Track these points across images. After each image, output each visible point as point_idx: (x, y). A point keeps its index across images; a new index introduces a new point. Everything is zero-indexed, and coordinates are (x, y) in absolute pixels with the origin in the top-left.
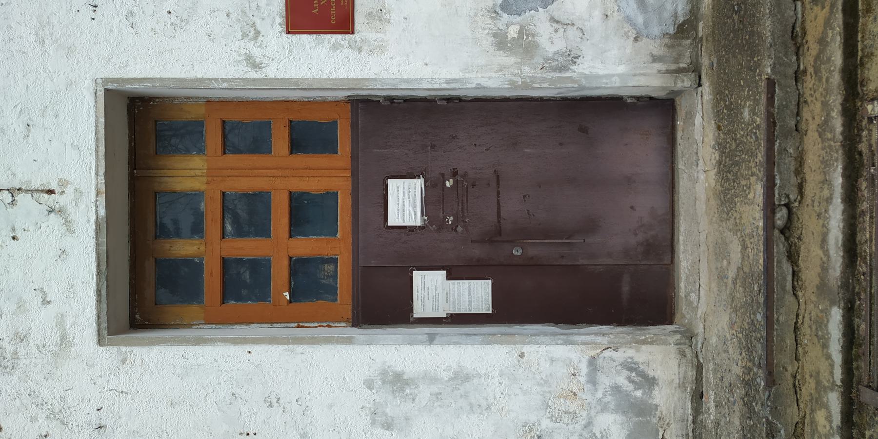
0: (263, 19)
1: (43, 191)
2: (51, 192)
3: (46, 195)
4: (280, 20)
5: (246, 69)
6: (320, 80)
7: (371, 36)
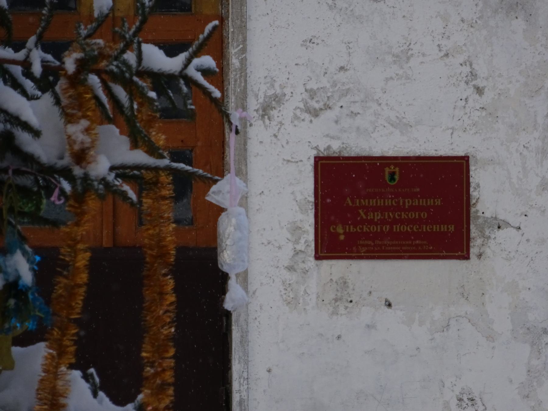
0: (337, 122)
5: (261, 95)
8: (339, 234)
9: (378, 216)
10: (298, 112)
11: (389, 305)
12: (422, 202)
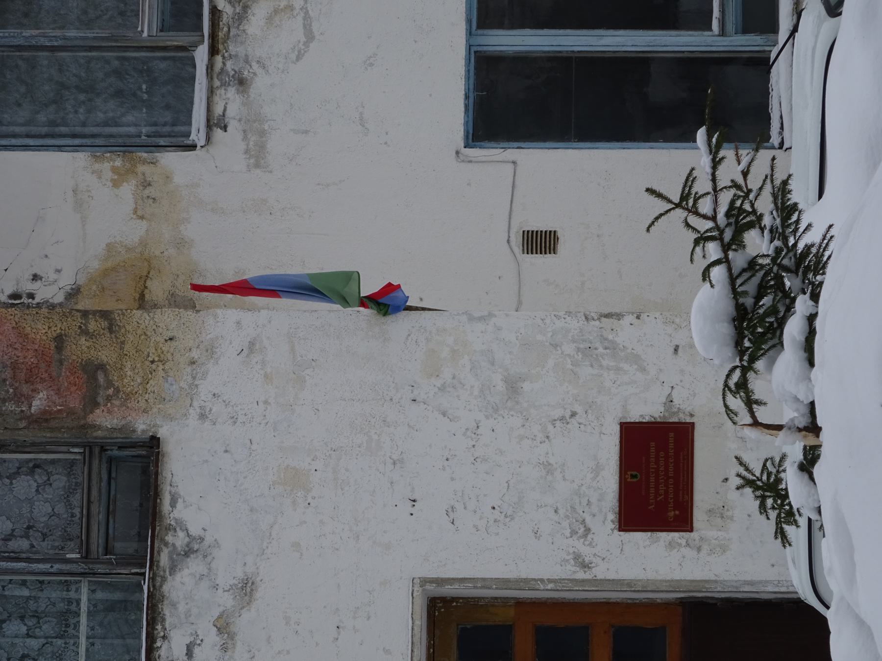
4: (612, 516)
5: (573, 569)
6: (654, 582)
8: (675, 514)
9: (662, 488)
10: (587, 543)
11: (727, 479)
12: (653, 455)
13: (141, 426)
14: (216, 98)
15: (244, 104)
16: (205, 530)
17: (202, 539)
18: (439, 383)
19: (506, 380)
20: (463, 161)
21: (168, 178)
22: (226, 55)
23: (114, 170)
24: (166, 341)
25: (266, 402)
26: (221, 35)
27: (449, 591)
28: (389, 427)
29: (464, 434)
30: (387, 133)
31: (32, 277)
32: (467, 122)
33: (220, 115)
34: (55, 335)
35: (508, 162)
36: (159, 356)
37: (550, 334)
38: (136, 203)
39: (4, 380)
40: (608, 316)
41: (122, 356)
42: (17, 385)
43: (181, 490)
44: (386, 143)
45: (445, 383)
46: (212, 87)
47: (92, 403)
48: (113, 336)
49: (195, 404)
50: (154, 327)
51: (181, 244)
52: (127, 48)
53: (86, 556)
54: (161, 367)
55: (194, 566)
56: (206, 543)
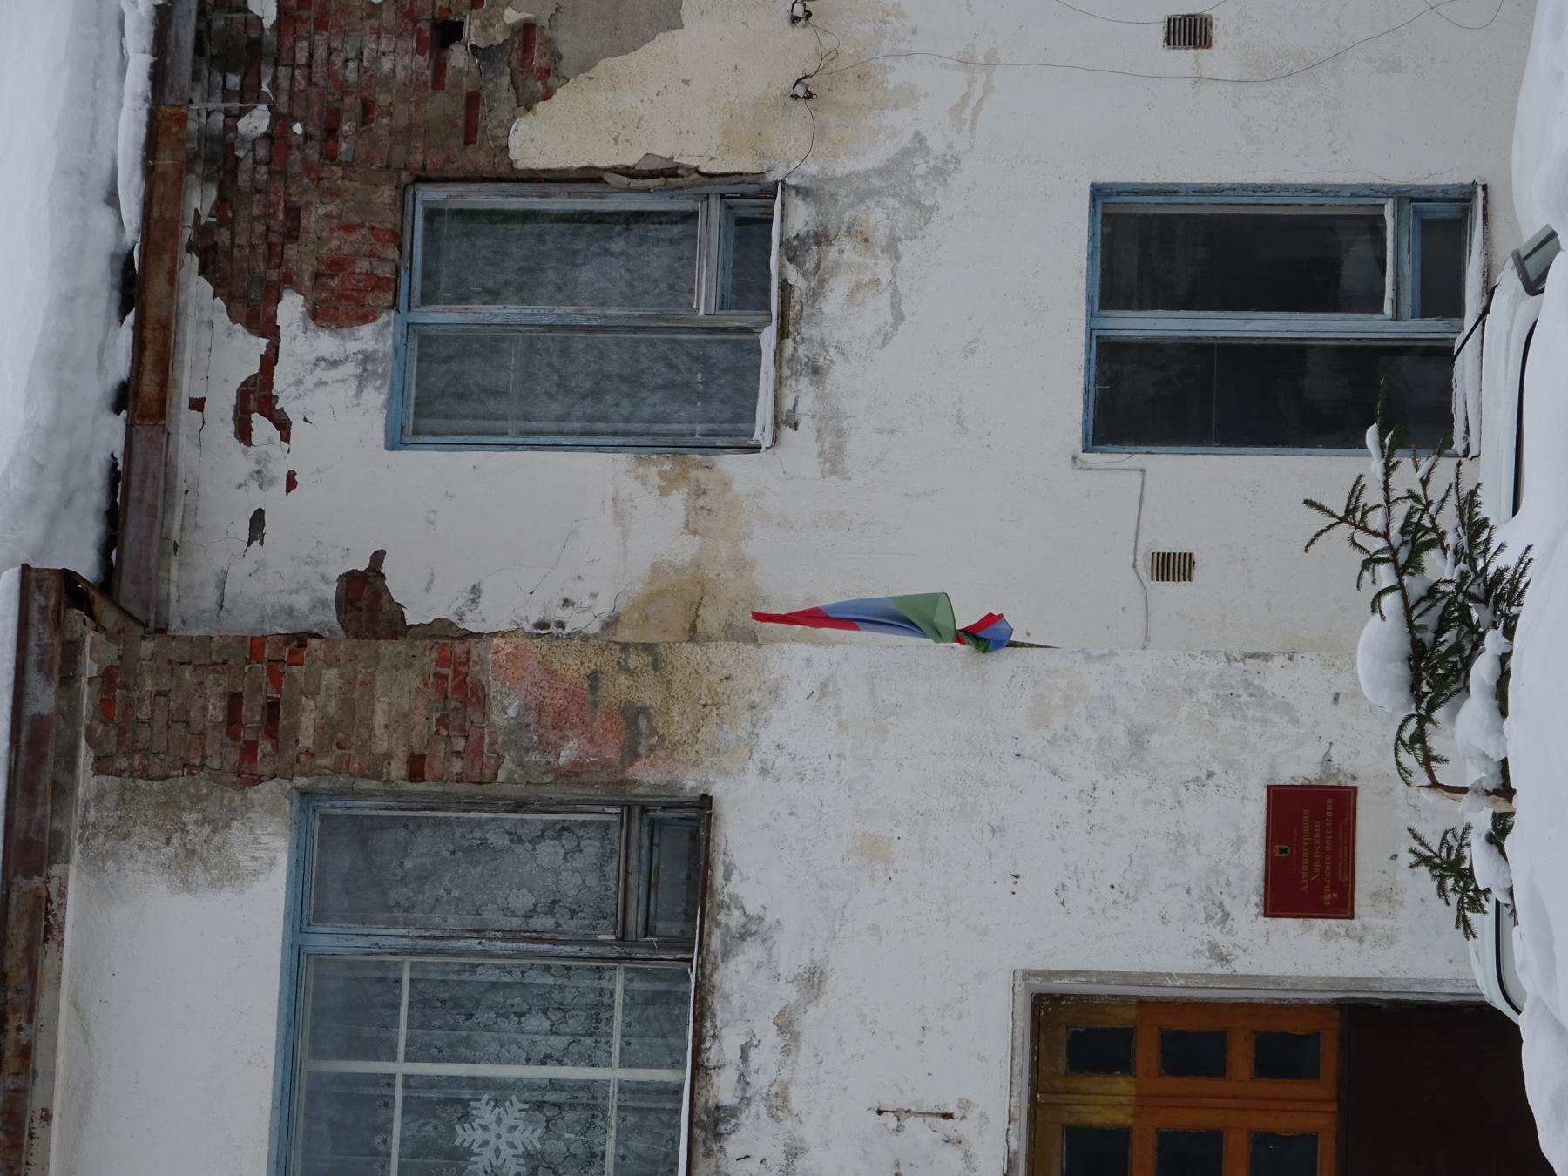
0: (1234, 897)
1: (937, 1115)
2: (947, 1116)
3: (941, 1120)
4: (1256, 899)
6: (1307, 979)
7: (1376, 922)
8: (1332, 898)
9: (1317, 865)
10: (1224, 930)
11: (1395, 856)
12: (1306, 825)
13: (690, 783)
14: (785, 390)
15: (818, 398)
16: (765, 908)
17: (761, 919)
18: (1048, 735)
19: (1129, 732)
20: (1081, 468)
21: (726, 485)
22: (798, 338)
23: (662, 475)
24: (721, 680)
25: (840, 756)
26: (792, 314)
27: (1056, 986)
28: (987, 786)
29: (1078, 798)
30: (990, 434)
31: (562, 603)
32: (1087, 421)
33: (789, 411)
34: (589, 672)
35: (1136, 470)
36: (713, 699)
37: (1183, 678)
38: (687, 515)
39: (528, 725)
40: (1254, 656)
41: (669, 697)
42: (542, 731)
43: (738, 859)
44: (988, 446)
45: (1055, 735)
46: (781, 377)
47: (631, 753)
48: (658, 673)
49: (755, 756)
50: (707, 664)
51: (741, 564)
52: (678, 329)
53: (622, 938)
54: (715, 712)
55: (751, 952)
56: (766, 924)
